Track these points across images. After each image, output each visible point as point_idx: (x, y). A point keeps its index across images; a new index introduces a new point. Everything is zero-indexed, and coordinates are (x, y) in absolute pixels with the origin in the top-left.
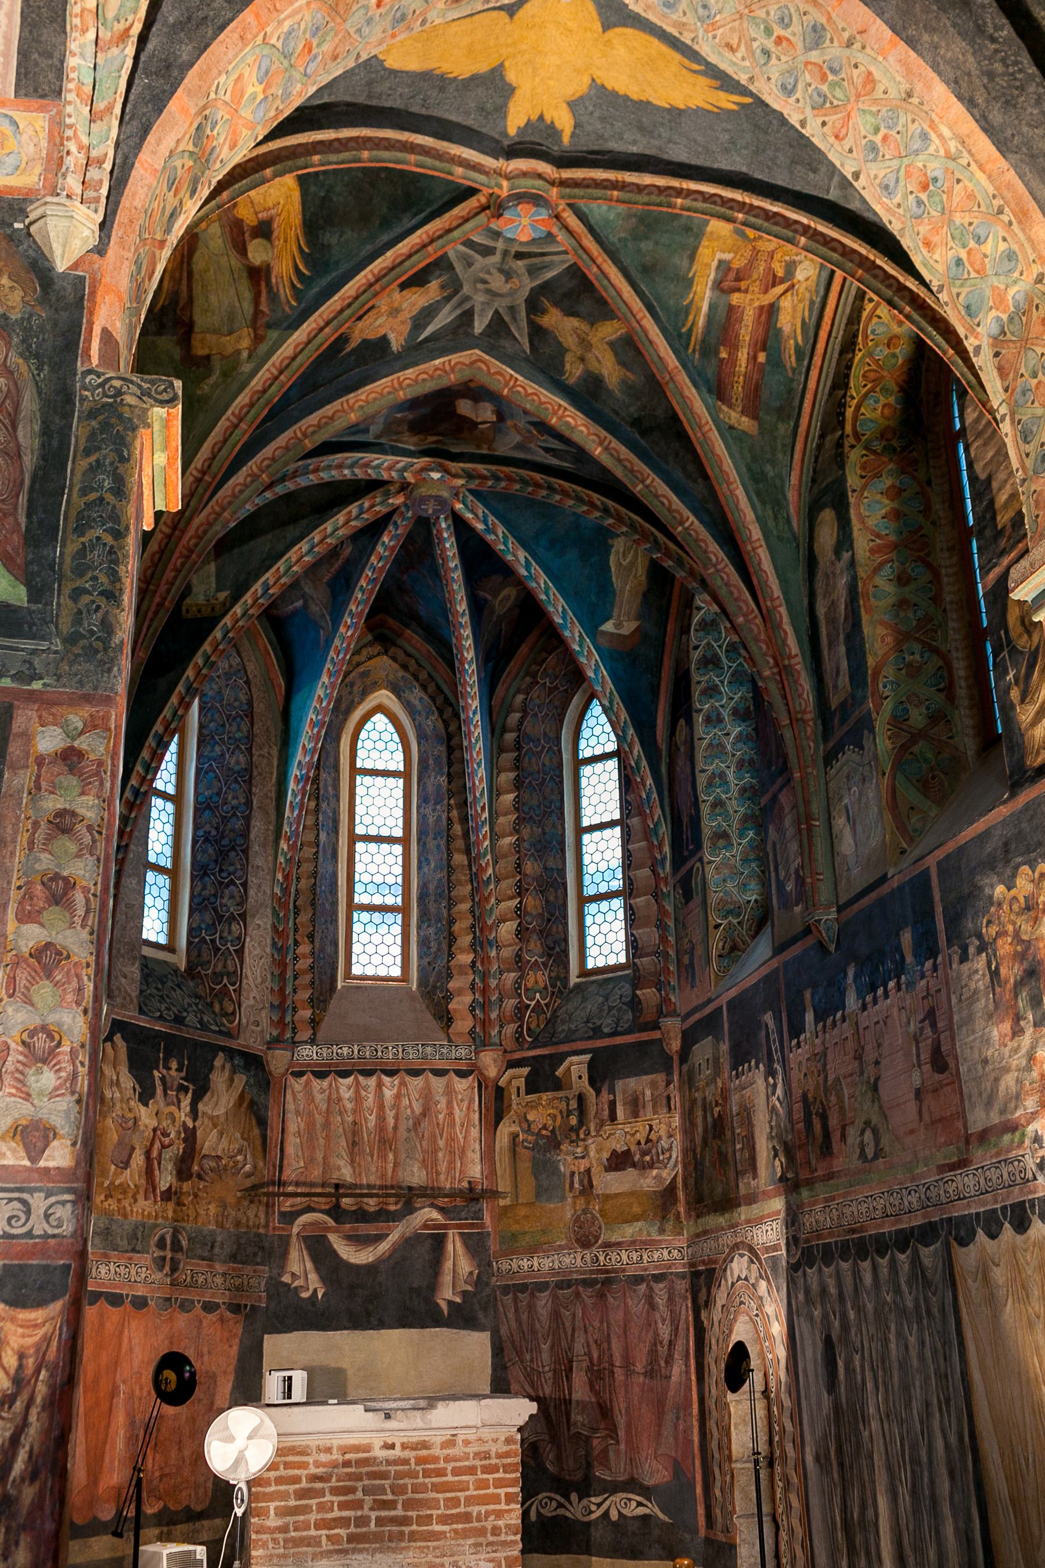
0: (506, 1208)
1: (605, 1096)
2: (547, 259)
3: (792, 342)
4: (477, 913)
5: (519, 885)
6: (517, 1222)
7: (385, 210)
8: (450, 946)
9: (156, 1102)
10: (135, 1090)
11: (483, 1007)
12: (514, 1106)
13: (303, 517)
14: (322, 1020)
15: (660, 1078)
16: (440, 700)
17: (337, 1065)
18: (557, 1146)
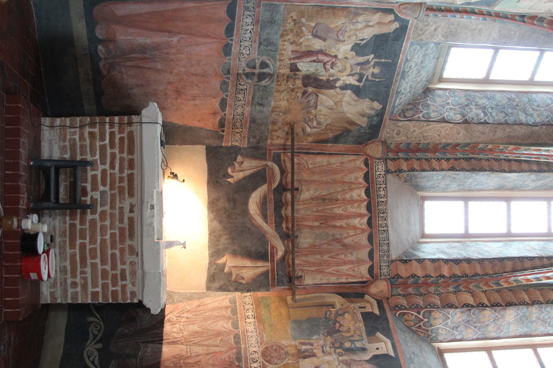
6: (276, 308)
9: (353, 58)
10: (362, 40)
11: (416, 283)
12: (352, 305)
14: (400, 179)
17: (373, 188)
18: (330, 334)
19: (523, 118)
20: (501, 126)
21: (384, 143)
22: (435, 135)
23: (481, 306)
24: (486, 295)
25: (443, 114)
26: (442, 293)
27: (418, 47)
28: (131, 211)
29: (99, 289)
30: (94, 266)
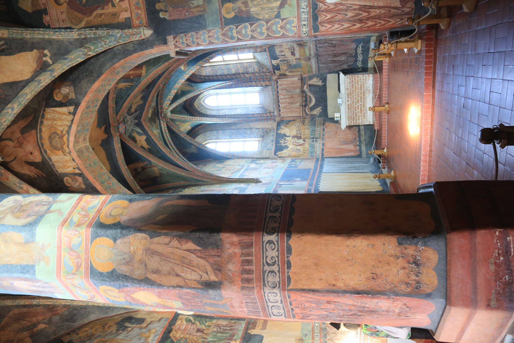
0: (303, 73)
1: (280, 57)
15: (276, 47)
18: (290, 65)
19: (233, 131)
21: (275, 121)
23: (243, 74)
28: (348, 100)
29: (357, 79)
30: (358, 85)
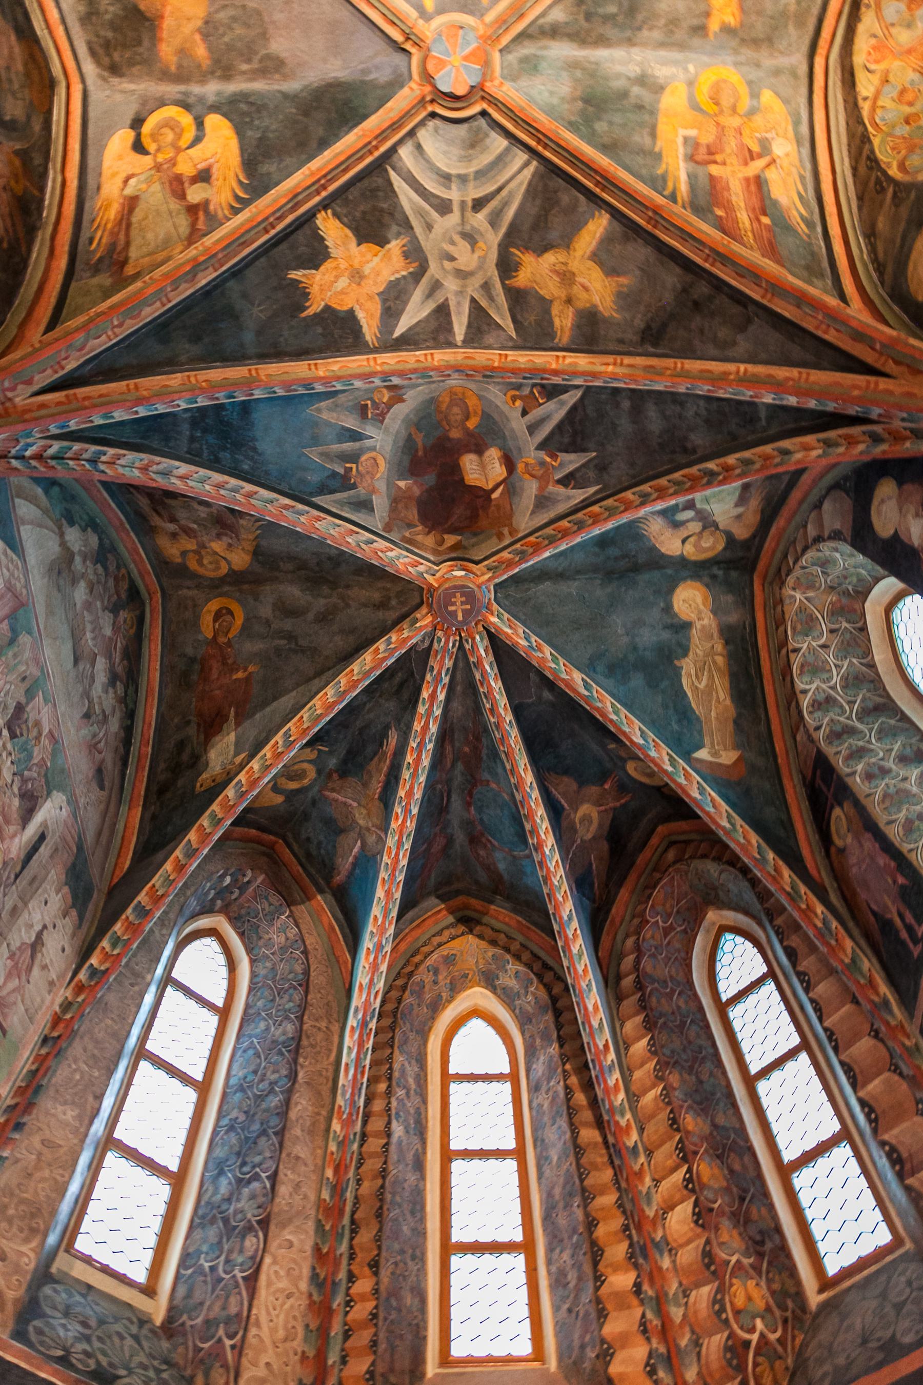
2: (504, 193)
3: (795, 213)
4: (628, 1206)
5: (681, 1148)
7: (321, 132)
8: (595, 1264)
13: (329, 669)
16: (537, 966)
19: (274, 1101)
20: (287, 1143)
22: (286, 1306)
24: (664, 1178)
25: (237, 1282)
26: (681, 1284)
27: (37, 1323)
